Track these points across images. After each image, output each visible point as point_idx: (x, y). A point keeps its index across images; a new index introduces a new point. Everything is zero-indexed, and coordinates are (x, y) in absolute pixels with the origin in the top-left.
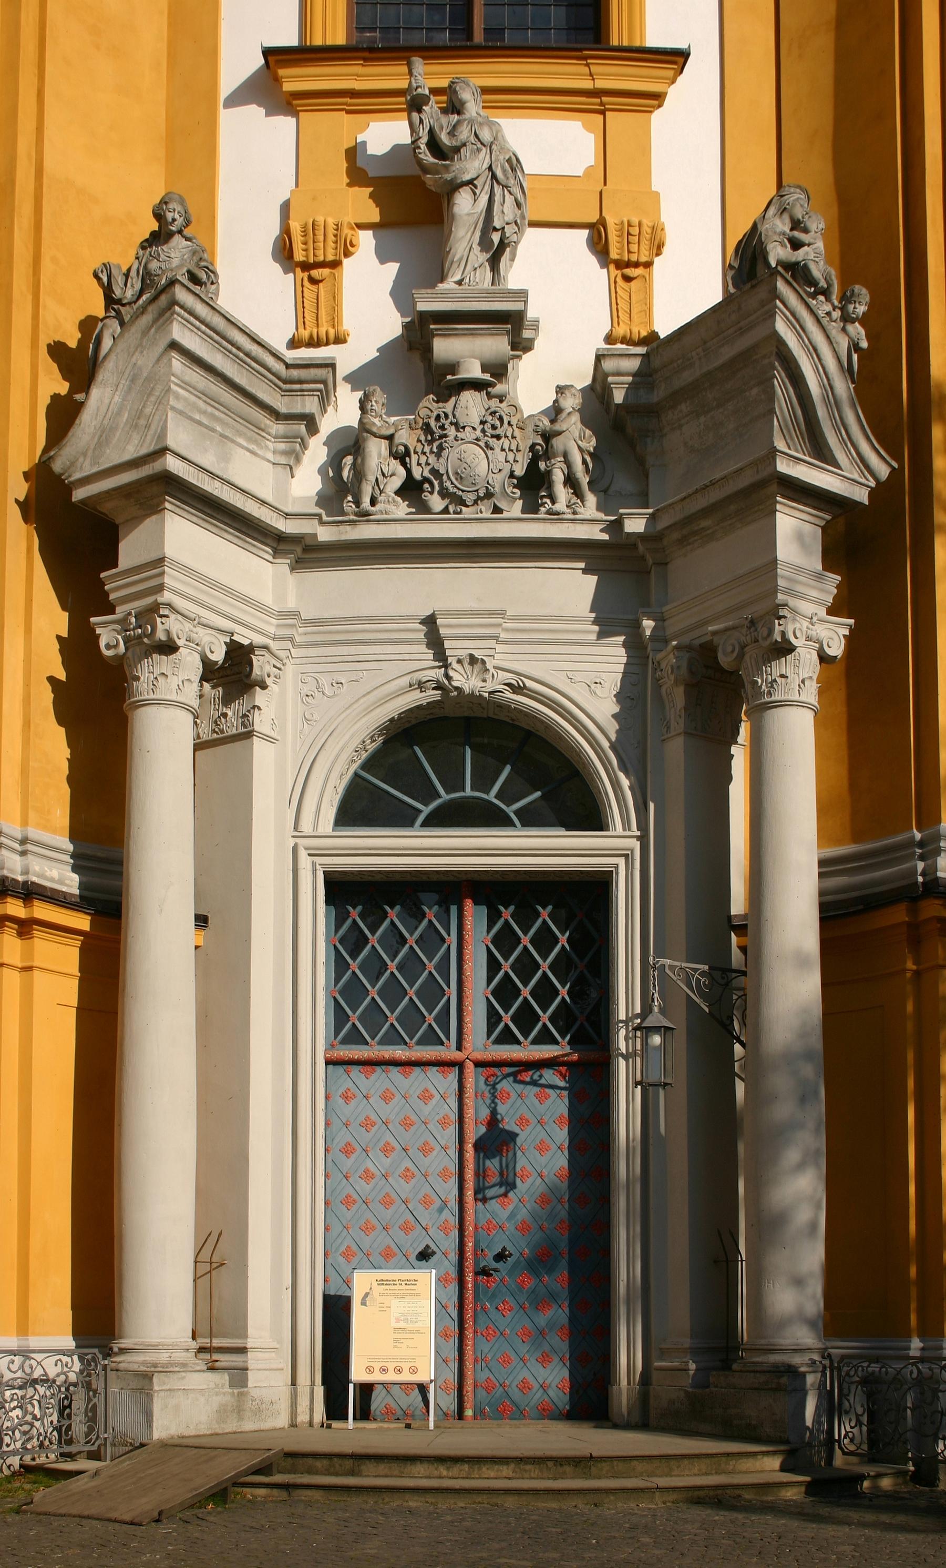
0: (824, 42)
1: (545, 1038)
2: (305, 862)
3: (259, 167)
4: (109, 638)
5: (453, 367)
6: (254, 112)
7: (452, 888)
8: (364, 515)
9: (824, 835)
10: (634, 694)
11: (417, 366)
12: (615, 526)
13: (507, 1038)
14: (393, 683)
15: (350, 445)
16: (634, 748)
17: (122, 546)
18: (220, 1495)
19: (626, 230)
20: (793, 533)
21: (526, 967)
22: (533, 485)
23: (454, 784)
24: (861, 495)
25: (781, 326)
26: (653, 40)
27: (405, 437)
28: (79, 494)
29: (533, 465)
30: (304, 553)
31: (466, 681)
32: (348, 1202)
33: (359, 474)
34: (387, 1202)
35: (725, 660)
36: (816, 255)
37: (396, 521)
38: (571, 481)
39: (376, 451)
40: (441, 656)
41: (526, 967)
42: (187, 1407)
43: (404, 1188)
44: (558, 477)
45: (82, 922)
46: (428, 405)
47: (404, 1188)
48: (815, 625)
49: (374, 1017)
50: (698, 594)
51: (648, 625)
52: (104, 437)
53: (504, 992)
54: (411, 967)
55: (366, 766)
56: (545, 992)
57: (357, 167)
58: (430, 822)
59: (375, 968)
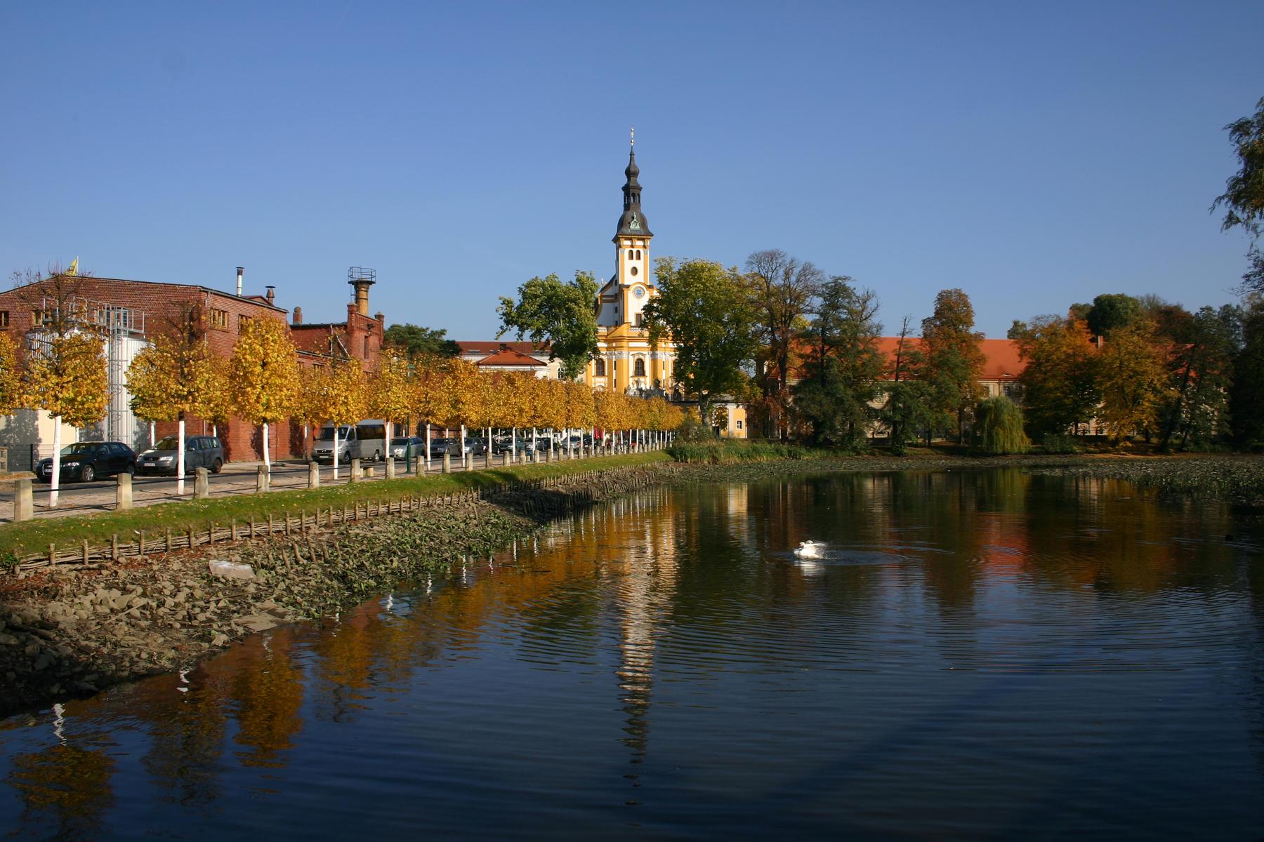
3: (631, 380)
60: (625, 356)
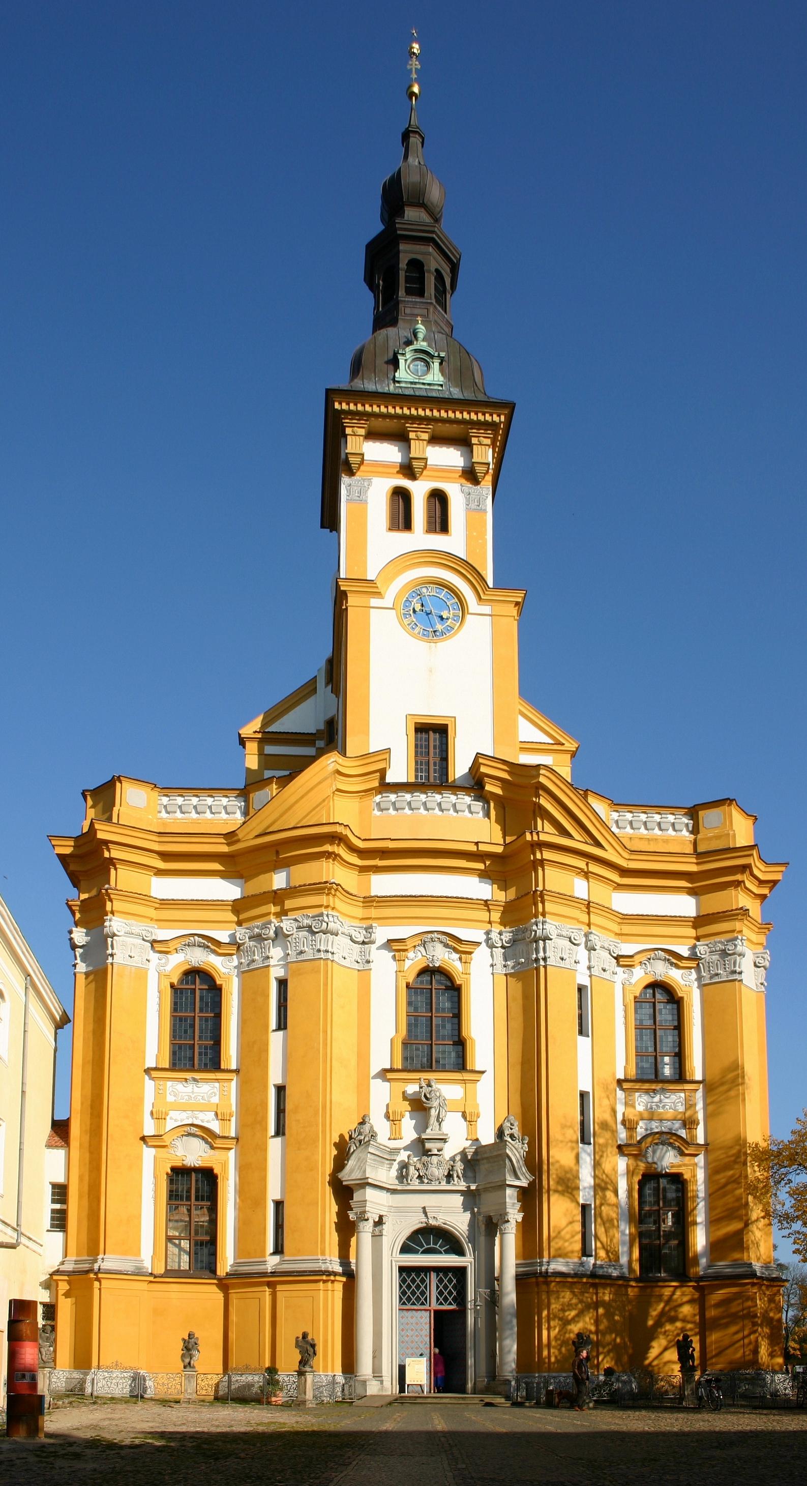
0: (519, 1068)
1: (450, 1304)
2: (394, 1264)
3: (381, 1095)
4: (352, 1216)
5: (430, 1150)
6: (379, 1081)
7: (427, 1270)
8: (409, 1184)
9: (517, 1257)
10: (472, 1224)
11: (421, 1147)
12: (469, 1187)
13: (441, 1304)
14: (416, 1222)
15: (404, 1166)
16: (472, 1238)
17: (355, 1195)
18: (390, 1404)
19: (471, 1114)
20: (511, 1195)
21: (446, 1287)
22: (449, 1177)
23: (428, 1244)
24: (525, 1185)
25: (508, 1151)
26: (477, 1069)
27: (418, 1166)
28: (344, 1183)
29: (449, 1173)
30: (394, 1191)
31: (432, 1222)
32: (403, 1342)
33: (407, 1174)
34: (412, 1342)
35: (495, 1221)
36: (516, 1131)
37: (415, 1185)
38: (458, 1176)
39: (412, 1169)
40: (426, 1215)
41: (446, 1287)
42: (373, 1389)
43: (416, 1339)
44: (455, 1176)
45: (344, 1279)
46: (425, 1158)
47: (416, 1339)
48: (515, 1215)
49: (409, 1299)
50: (488, 1205)
51: (476, 1210)
52: (352, 1171)
53: (441, 1293)
54: (418, 1287)
55: (407, 1239)
56: (450, 1293)
57: (405, 1097)
58: (423, 1252)
59: (409, 1287)
60: (342, 949)
